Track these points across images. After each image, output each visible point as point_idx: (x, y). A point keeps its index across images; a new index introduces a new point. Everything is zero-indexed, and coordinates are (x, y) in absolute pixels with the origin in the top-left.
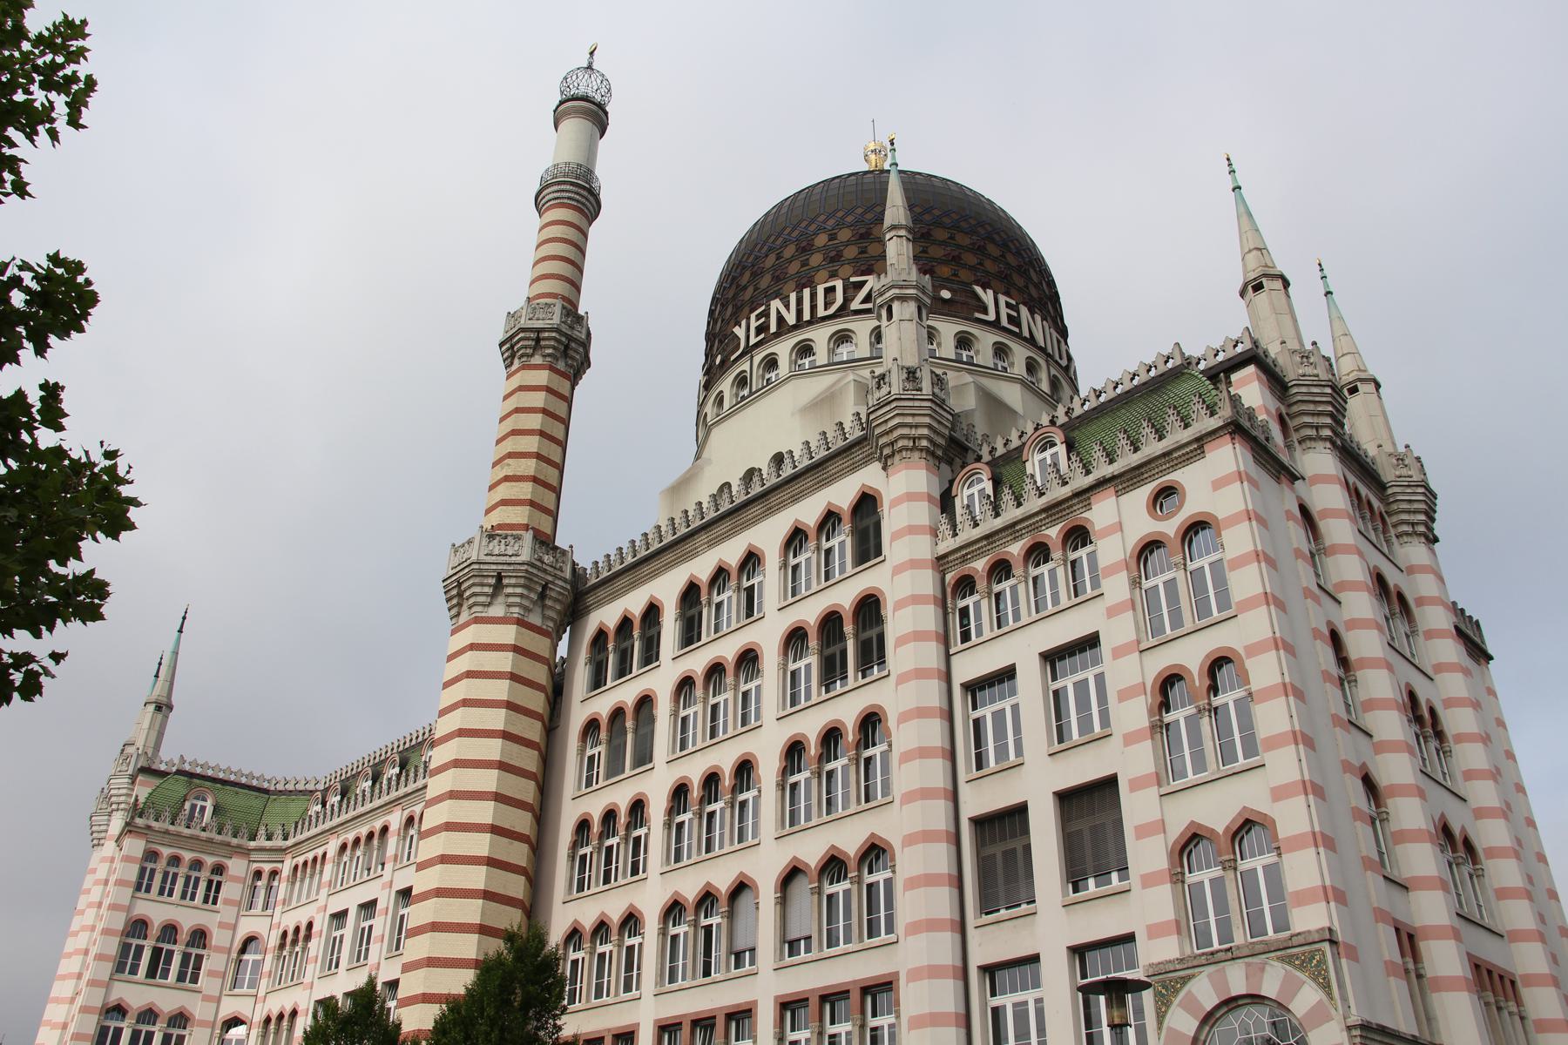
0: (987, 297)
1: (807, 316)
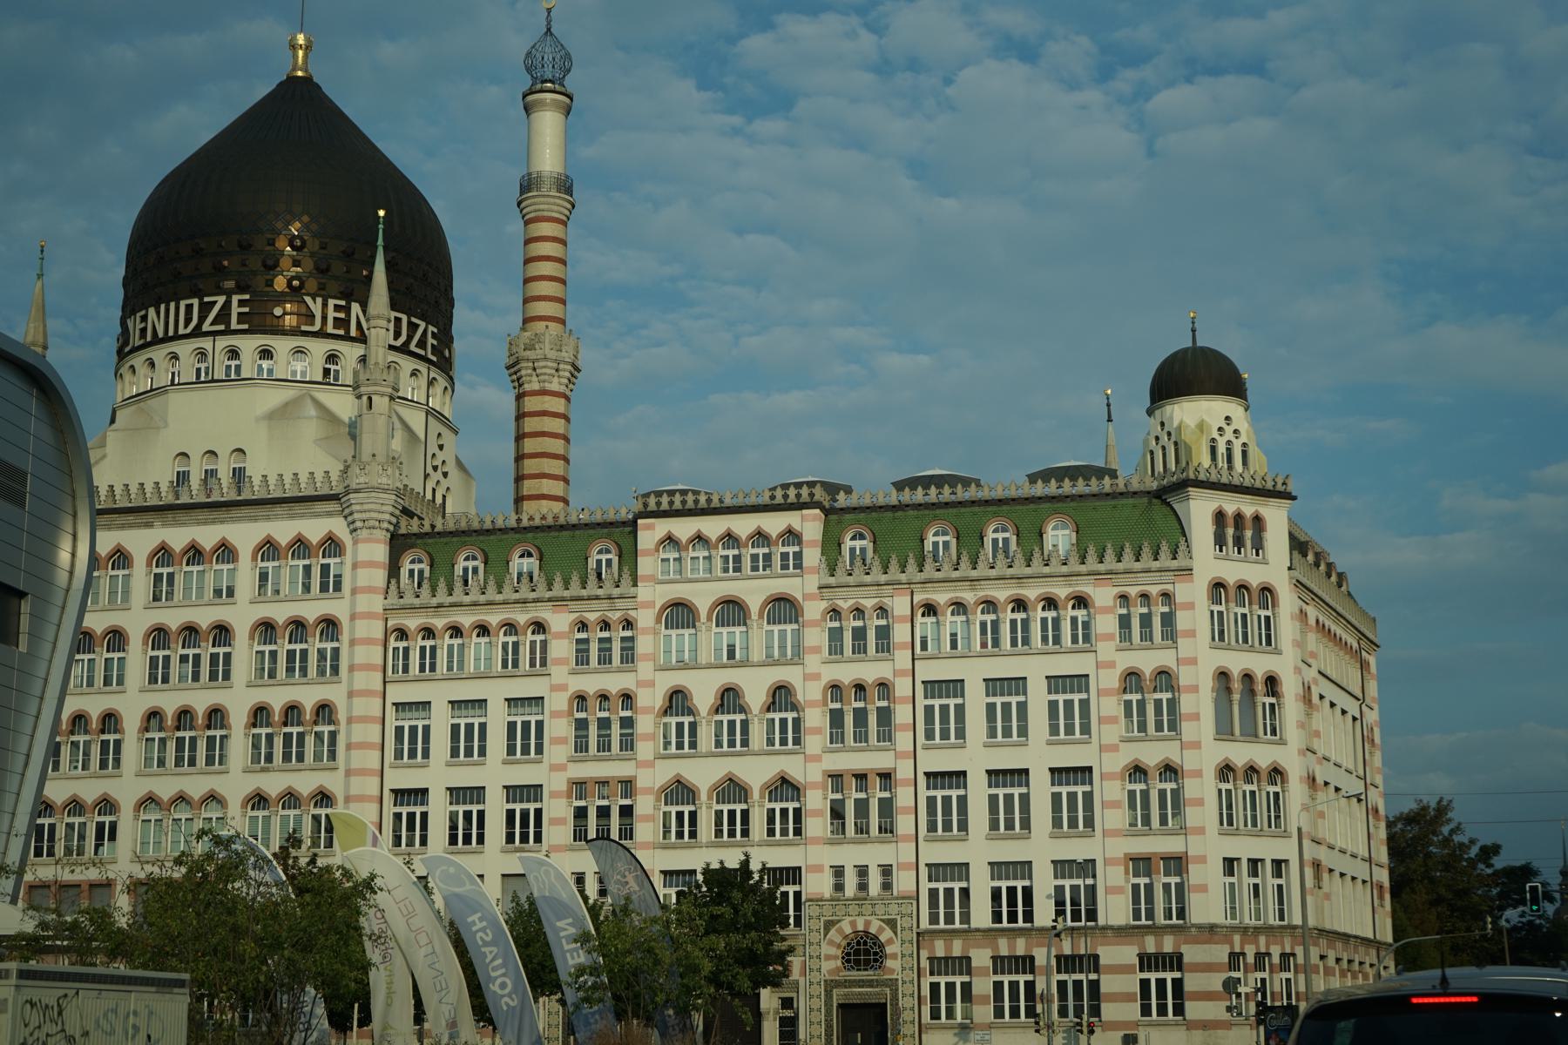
0: (316, 307)
1: (171, 333)
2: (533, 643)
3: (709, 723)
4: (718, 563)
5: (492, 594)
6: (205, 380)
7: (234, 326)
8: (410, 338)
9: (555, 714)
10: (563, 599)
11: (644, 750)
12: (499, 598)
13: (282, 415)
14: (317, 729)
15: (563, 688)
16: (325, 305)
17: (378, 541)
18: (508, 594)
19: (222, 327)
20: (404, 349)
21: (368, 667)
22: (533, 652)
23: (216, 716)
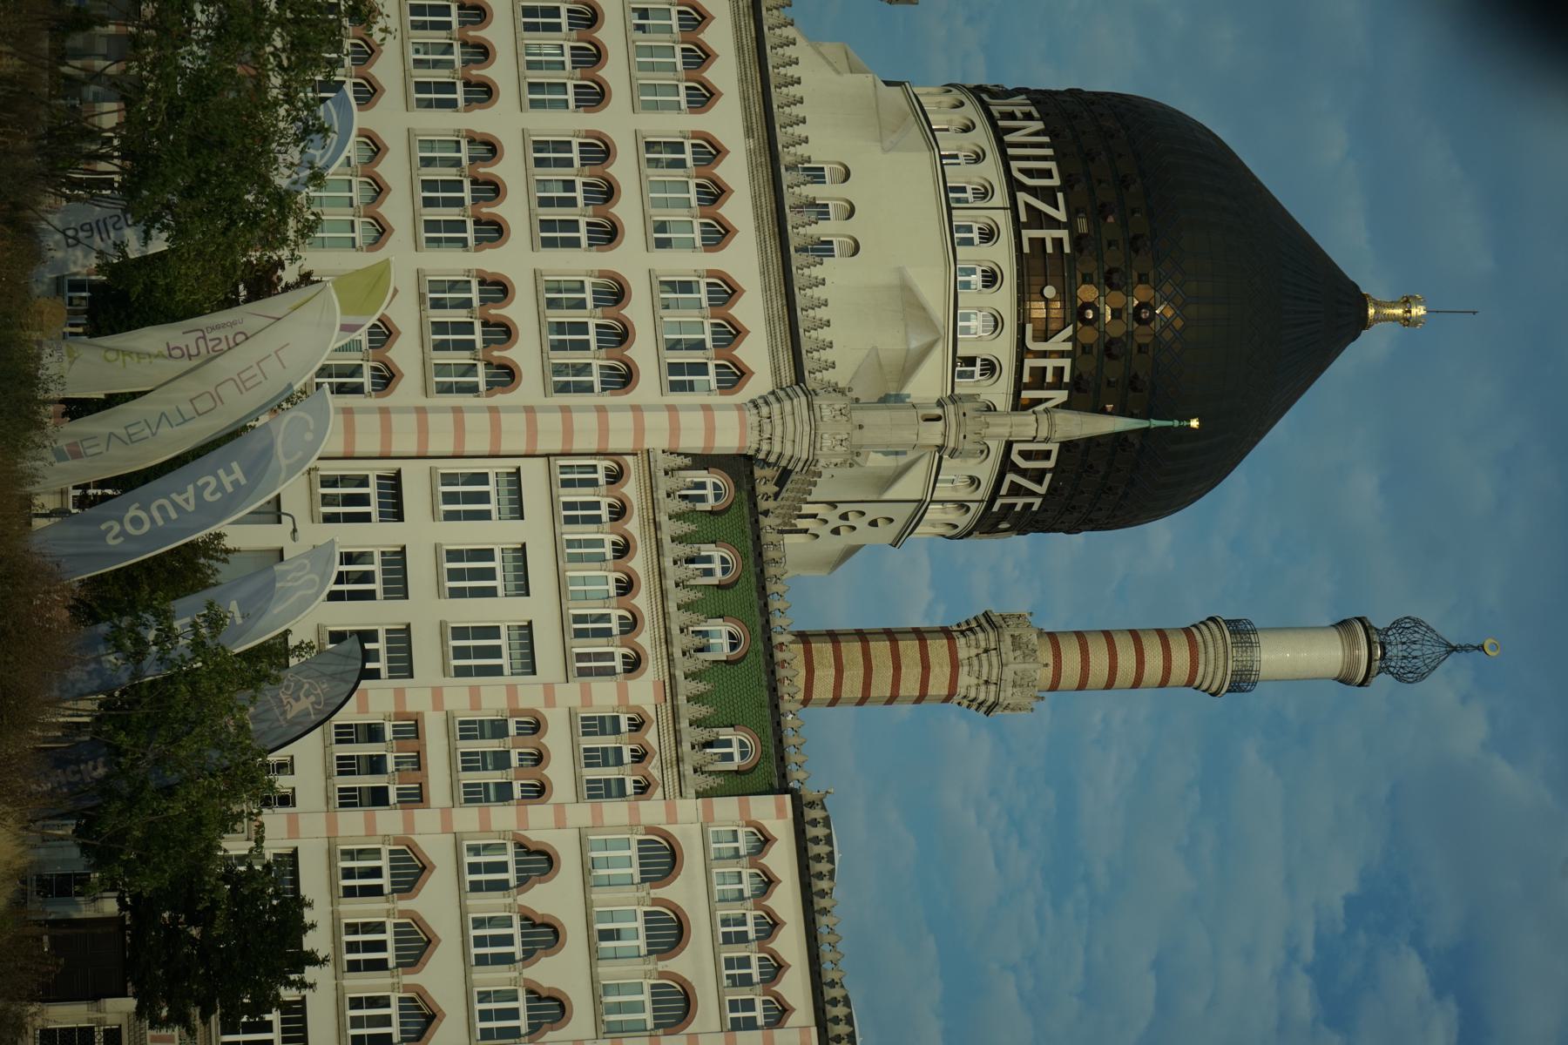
0: (1059, 342)
1: (1011, 151)
2: (611, 657)
3: (509, 907)
4: (734, 911)
5: (676, 596)
6: (950, 196)
7: (1027, 234)
8: (1023, 473)
9: (512, 691)
10: (674, 695)
11: (468, 819)
12: (672, 607)
13: (910, 303)
14: (481, 367)
15: (550, 701)
16: (1062, 354)
17: (743, 436)
18: (677, 619)
19: (1023, 218)
20: (1007, 465)
21: (568, 432)
22: (599, 656)
23: (493, 231)
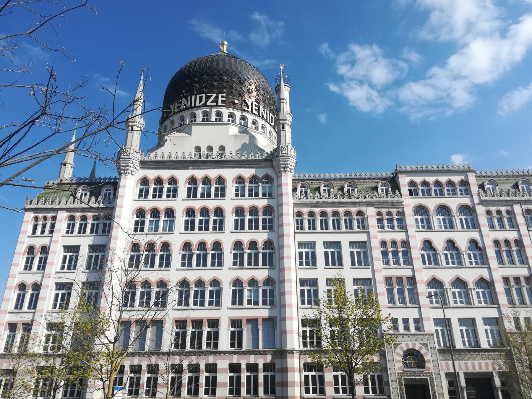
1: (193, 105)
19: (215, 104)
